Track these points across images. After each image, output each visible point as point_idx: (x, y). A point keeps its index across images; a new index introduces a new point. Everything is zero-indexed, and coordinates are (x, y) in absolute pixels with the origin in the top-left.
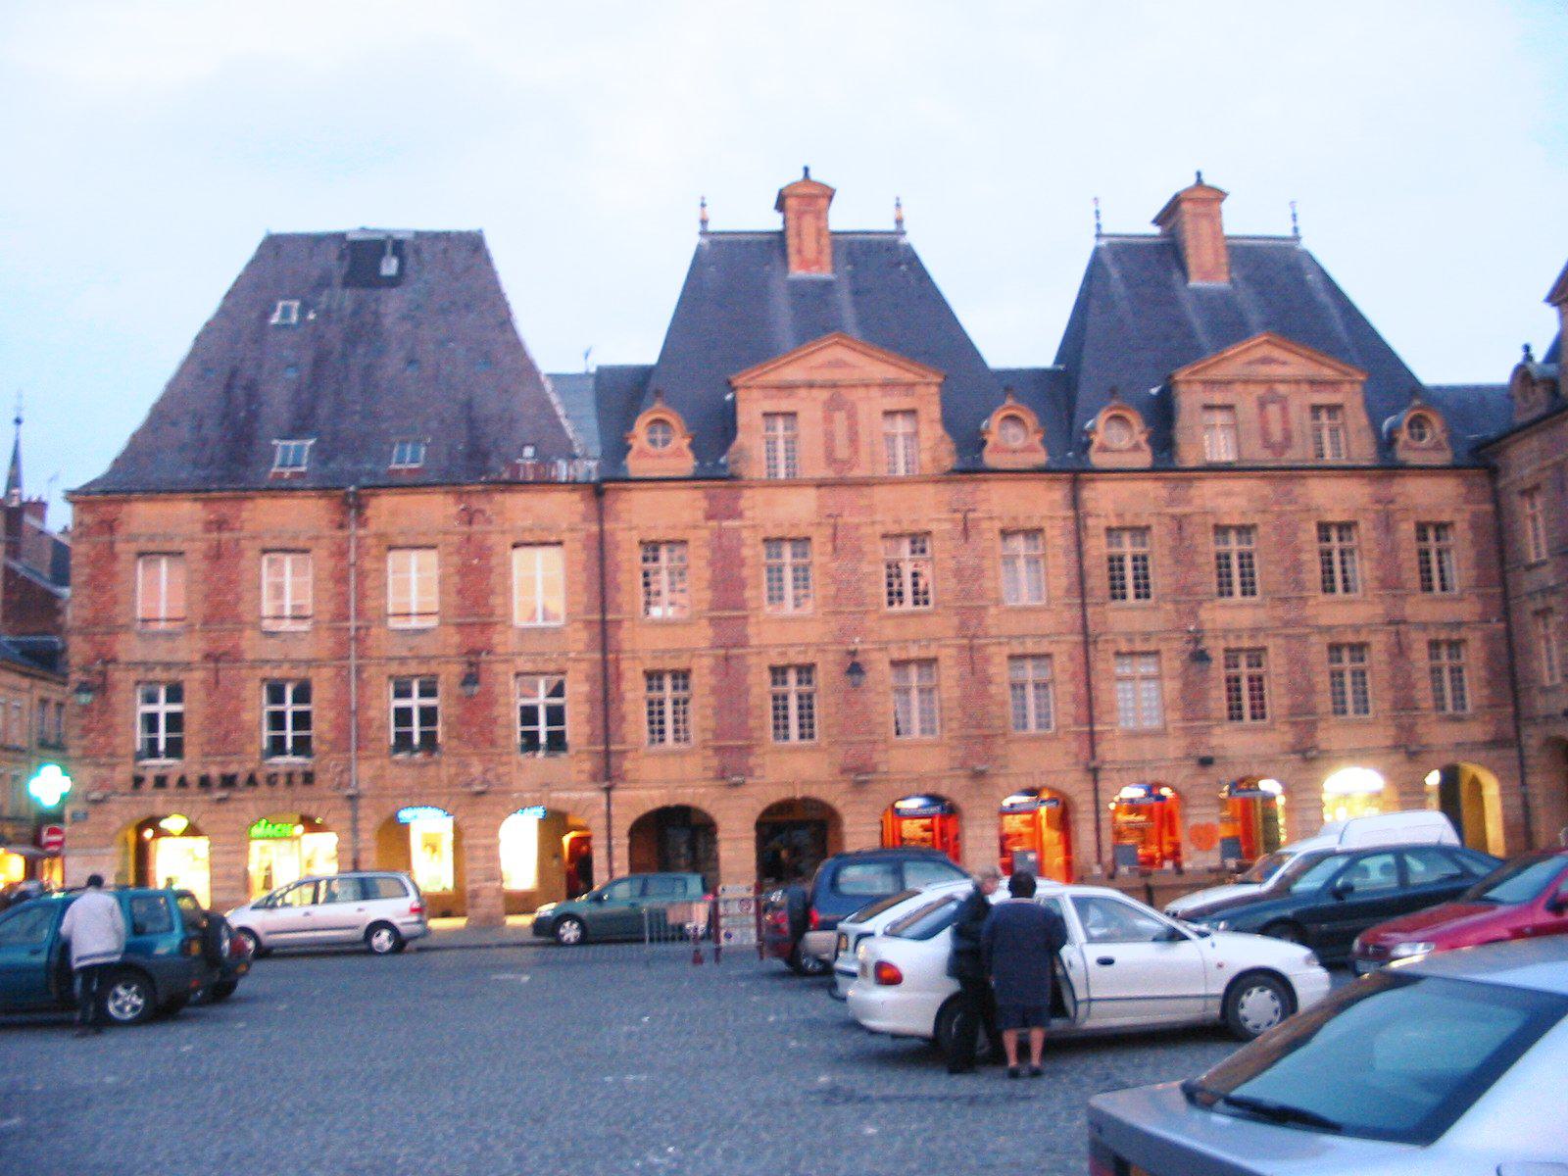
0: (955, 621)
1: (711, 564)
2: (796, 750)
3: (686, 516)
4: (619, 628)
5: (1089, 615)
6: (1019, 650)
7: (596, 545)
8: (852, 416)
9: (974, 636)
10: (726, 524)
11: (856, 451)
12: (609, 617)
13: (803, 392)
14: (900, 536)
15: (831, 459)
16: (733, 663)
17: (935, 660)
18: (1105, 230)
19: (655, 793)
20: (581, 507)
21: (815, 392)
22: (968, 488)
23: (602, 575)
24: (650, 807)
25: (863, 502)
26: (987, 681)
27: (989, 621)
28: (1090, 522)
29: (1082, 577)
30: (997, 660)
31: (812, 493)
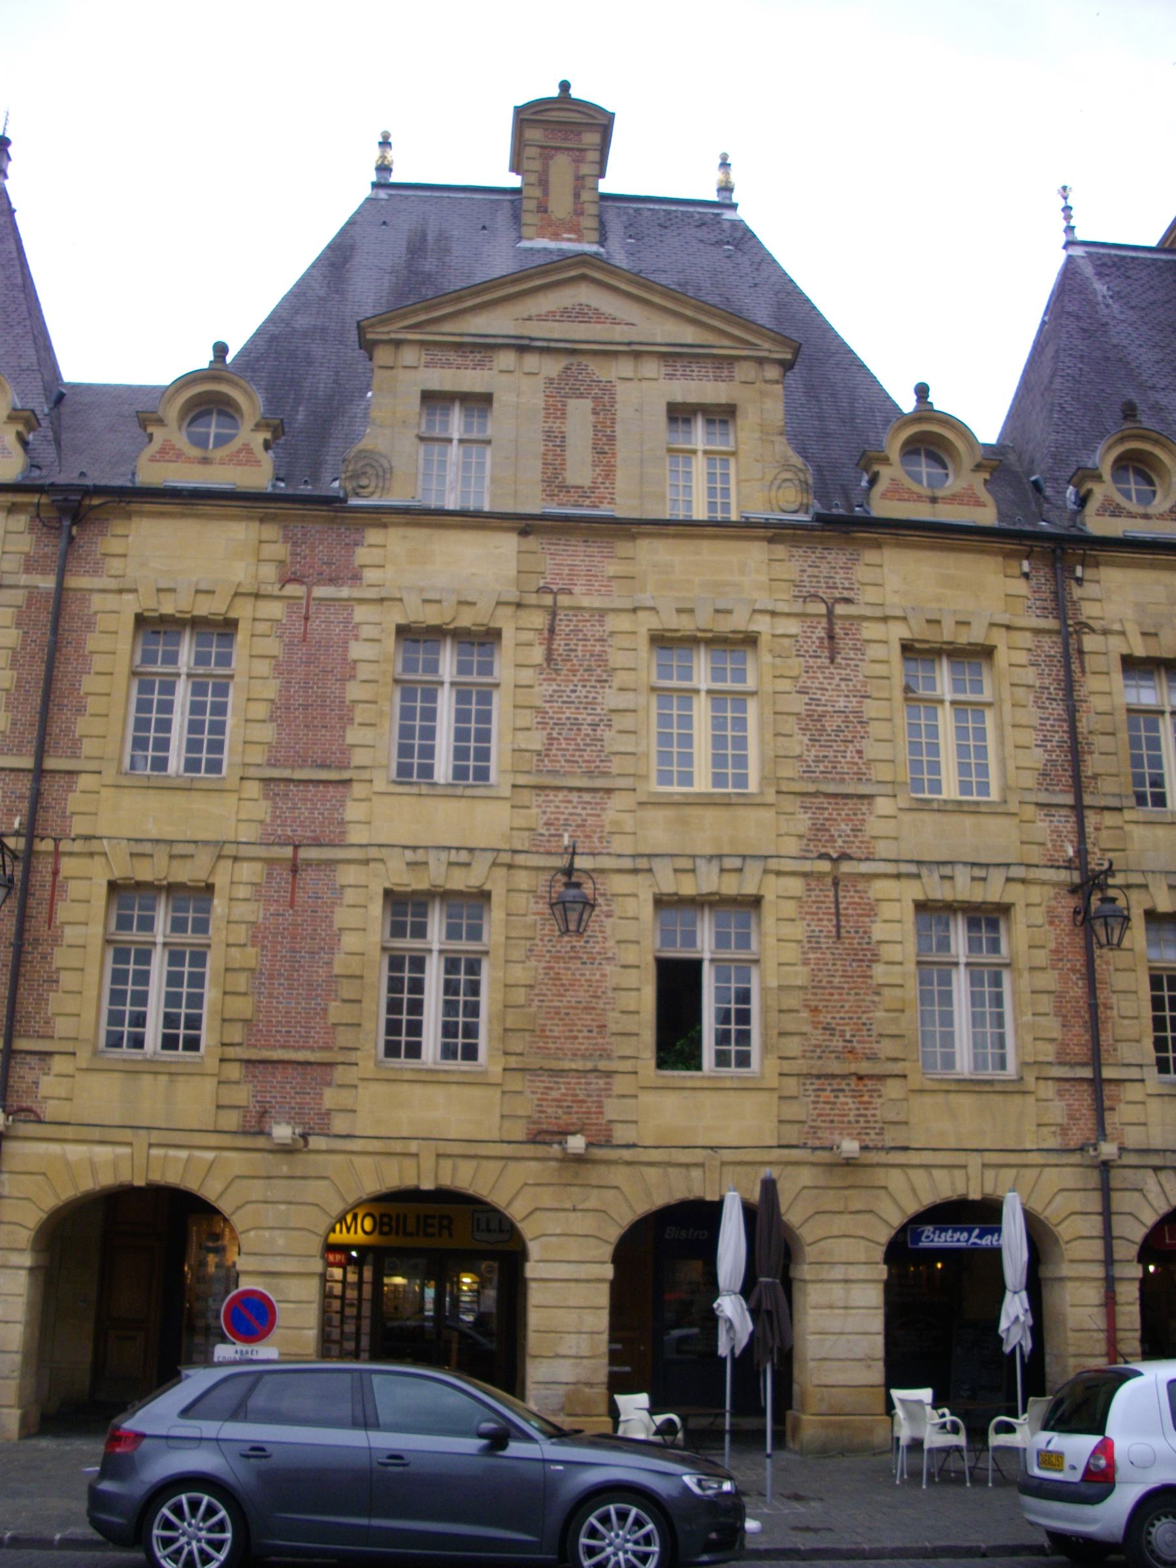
0: (803, 822)
1: (281, 668)
2: (431, 1078)
3: (241, 573)
4: (70, 789)
5: (1089, 830)
6: (939, 891)
7: (45, 617)
8: (604, 408)
9: (845, 857)
10: (320, 592)
11: (609, 473)
12: (50, 763)
13: (506, 359)
14: (691, 641)
15: (554, 483)
16: (308, 877)
17: (756, 902)
18: (1080, 235)
19: (103, 1153)
20: (24, 543)
21: (531, 361)
22: (837, 557)
23: (49, 679)
24: (88, 1184)
25: (612, 569)
26: (868, 955)
27: (874, 827)
28: (1090, 642)
29: (1075, 750)
30: (887, 911)
31: (507, 544)
